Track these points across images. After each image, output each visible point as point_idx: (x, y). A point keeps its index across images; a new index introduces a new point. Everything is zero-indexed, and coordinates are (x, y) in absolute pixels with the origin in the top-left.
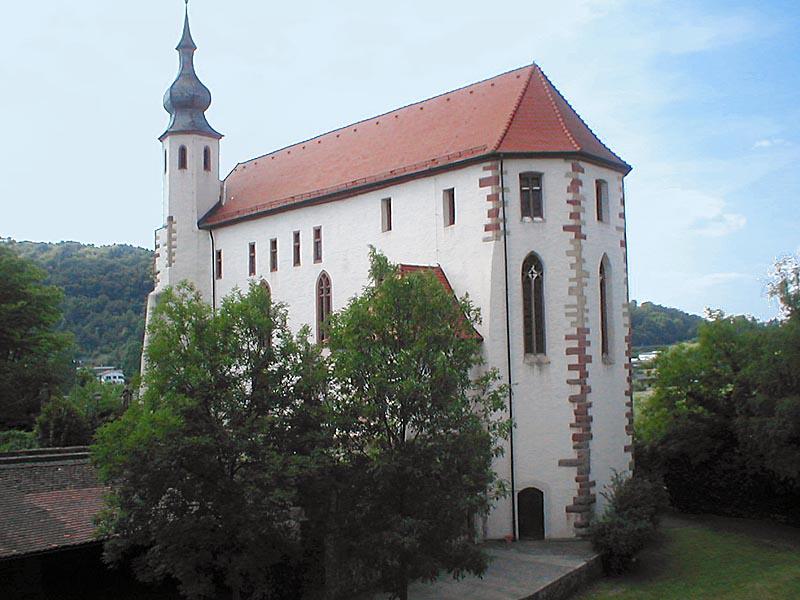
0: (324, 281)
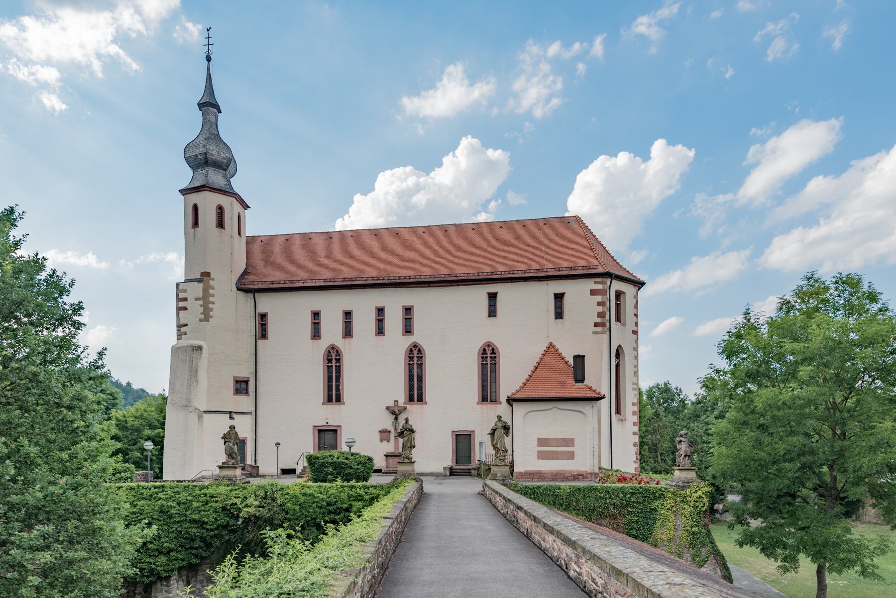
0: (415, 352)
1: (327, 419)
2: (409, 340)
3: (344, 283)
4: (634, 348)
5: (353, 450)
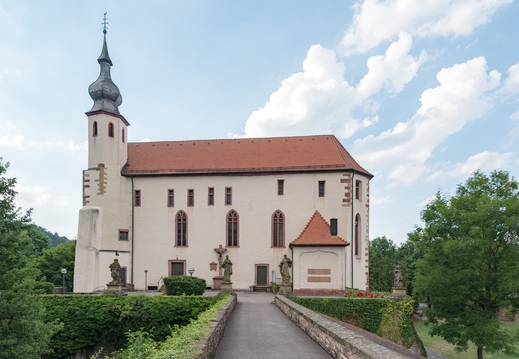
0: (233, 215)
2: (229, 208)
3: (189, 172)
4: (367, 215)
5: (193, 275)
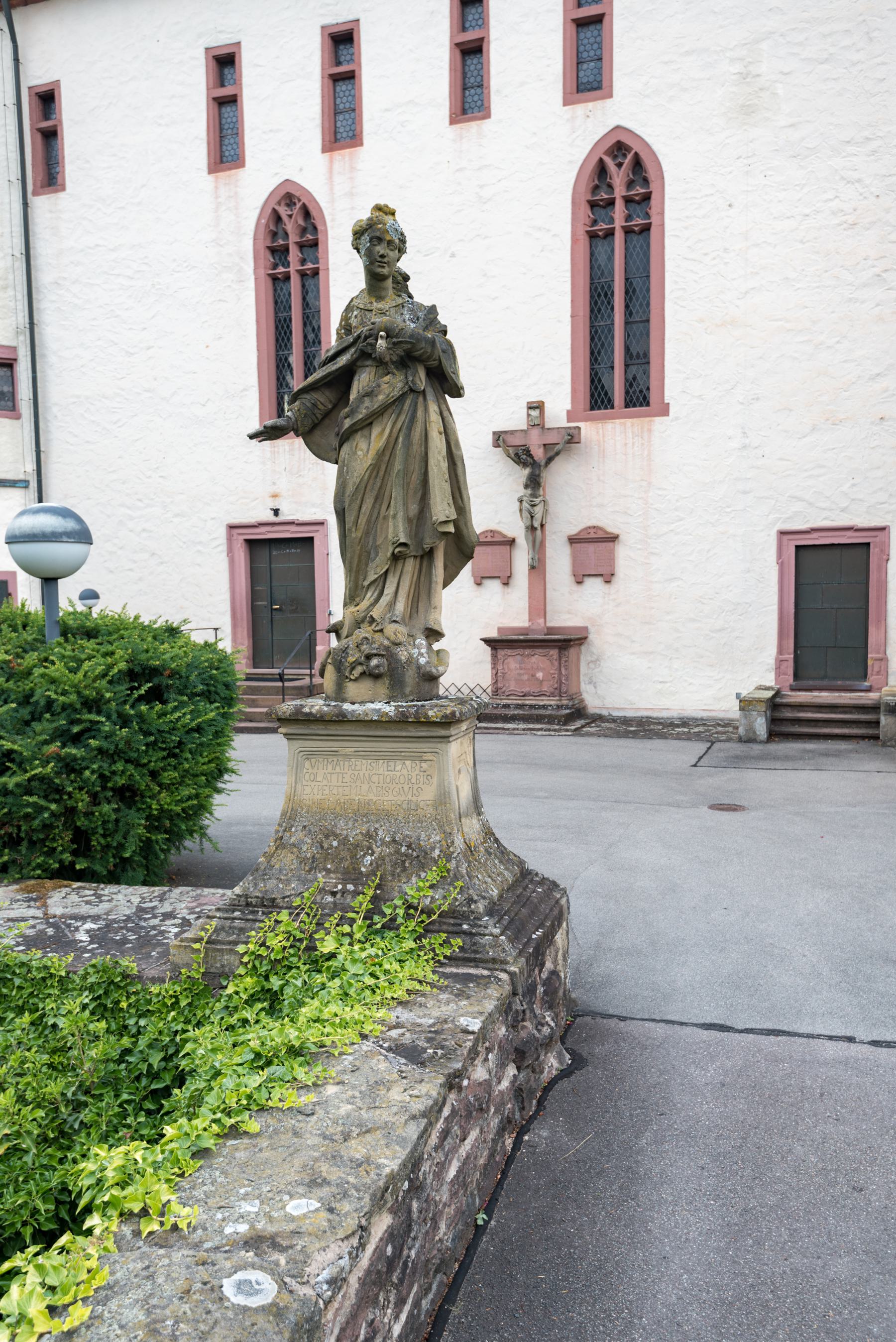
0: (618, 178)
1: (275, 496)
